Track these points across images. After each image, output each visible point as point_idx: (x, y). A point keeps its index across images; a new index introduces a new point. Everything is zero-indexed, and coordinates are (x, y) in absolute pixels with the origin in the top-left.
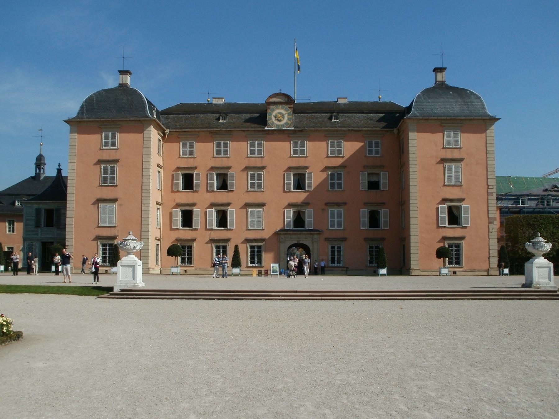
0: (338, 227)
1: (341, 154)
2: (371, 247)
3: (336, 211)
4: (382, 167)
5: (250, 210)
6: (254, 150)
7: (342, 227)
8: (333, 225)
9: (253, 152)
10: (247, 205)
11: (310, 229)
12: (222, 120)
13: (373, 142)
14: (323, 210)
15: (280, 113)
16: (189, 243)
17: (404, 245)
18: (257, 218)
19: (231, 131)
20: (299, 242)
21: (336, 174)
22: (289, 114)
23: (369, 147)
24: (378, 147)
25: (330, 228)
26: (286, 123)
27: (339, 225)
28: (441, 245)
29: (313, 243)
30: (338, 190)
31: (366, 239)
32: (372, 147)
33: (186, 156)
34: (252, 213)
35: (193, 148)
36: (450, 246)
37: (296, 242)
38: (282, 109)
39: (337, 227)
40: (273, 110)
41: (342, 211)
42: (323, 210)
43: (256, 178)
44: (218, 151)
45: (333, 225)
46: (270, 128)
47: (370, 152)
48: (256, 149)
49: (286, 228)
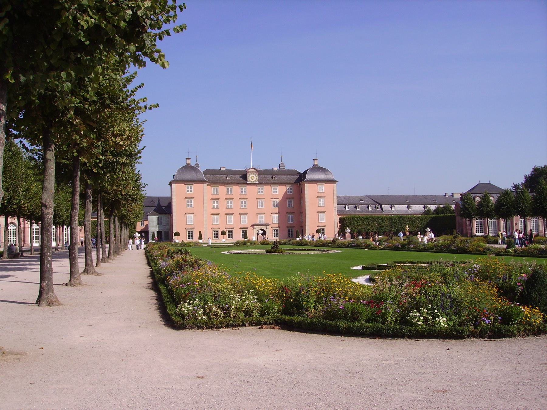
2: (289, 230)
4: (293, 198)
9: (242, 192)
15: (253, 176)
16: (217, 230)
17: (302, 229)
22: (256, 177)
26: (255, 181)
28: (318, 228)
29: (267, 228)
31: (287, 227)
36: (321, 229)
38: (254, 174)
40: (250, 175)
47: (288, 192)
48: (243, 191)
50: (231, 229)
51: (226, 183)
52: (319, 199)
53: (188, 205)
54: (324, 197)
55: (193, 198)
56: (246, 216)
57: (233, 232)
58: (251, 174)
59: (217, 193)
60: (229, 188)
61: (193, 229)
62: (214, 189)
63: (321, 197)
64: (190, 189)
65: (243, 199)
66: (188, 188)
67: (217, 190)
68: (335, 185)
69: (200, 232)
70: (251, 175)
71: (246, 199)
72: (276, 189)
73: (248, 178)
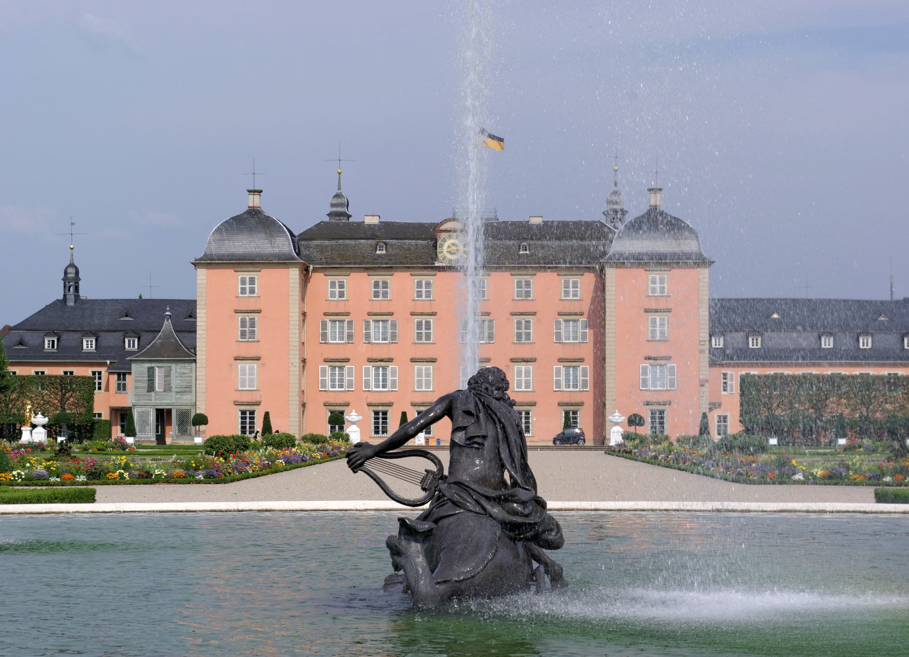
0: (525, 388)
1: (530, 296)
3: (523, 368)
5: (417, 366)
6: (421, 291)
10: (413, 360)
12: (380, 250)
13: (571, 280)
15: (453, 244)
18: (426, 376)
19: (392, 267)
21: (523, 322)
23: (565, 288)
24: (577, 287)
27: (527, 386)
30: (527, 342)
31: (560, 404)
32: (569, 288)
33: (335, 299)
34: (420, 371)
35: (343, 288)
39: (525, 388)
40: (444, 240)
42: (507, 366)
43: (424, 327)
44: (375, 292)
46: (441, 265)
47: (567, 293)
48: (424, 290)
50: (383, 405)
51: (371, 265)
52: (651, 316)
53: (243, 334)
54: (669, 311)
55: (259, 312)
56: (431, 366)
57: (389, 415)
58: (450, 237)
59: (341, 295)
60: (380, 279)
61: (258, 404)
62: (333, 284)
63: (656, 311)
64: (248, 286)
65: (422, 314)
66: (243, 282)
67: (341, 286)
68: (704, 273)
69: (267, 415)
70: (449, 242)
71: (433, 314)
72: (528, 284)
73: (439, 250)
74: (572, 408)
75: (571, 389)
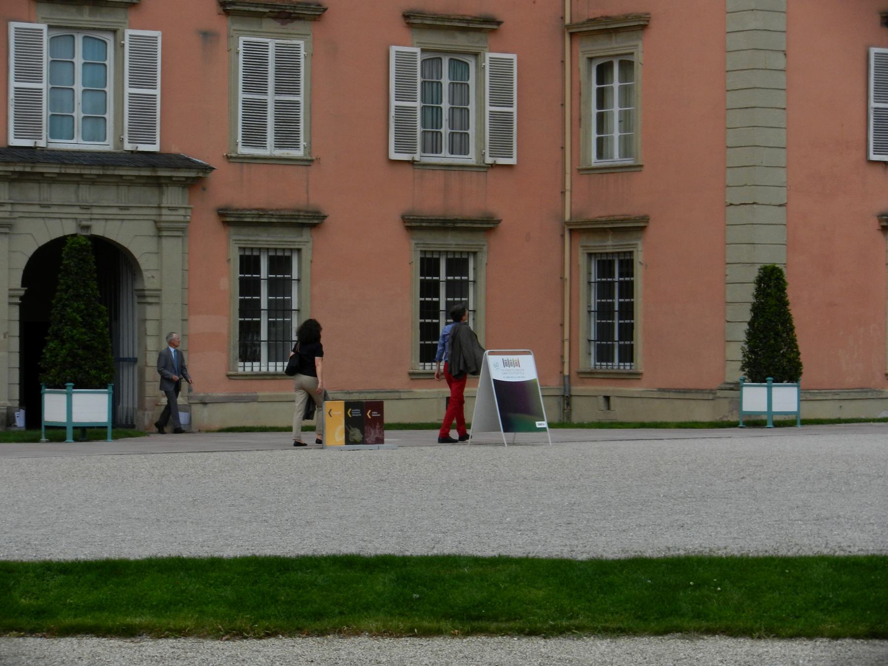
0: (279, 145)
2: (429, 266)
3: (272, 43)
7: (302, 143)
8: (254, 136)
11: (143, 148)
14: (207, 36)
20: (88, 227)
25: (243, 150)
29: (160, 231)
37: (69, 228)
39: (279, 145)
41: (302, 53)
42: (207, 36)
45: (254, 136)
49: (14, 142)
74: (453, 242)
75: (445, 157)
